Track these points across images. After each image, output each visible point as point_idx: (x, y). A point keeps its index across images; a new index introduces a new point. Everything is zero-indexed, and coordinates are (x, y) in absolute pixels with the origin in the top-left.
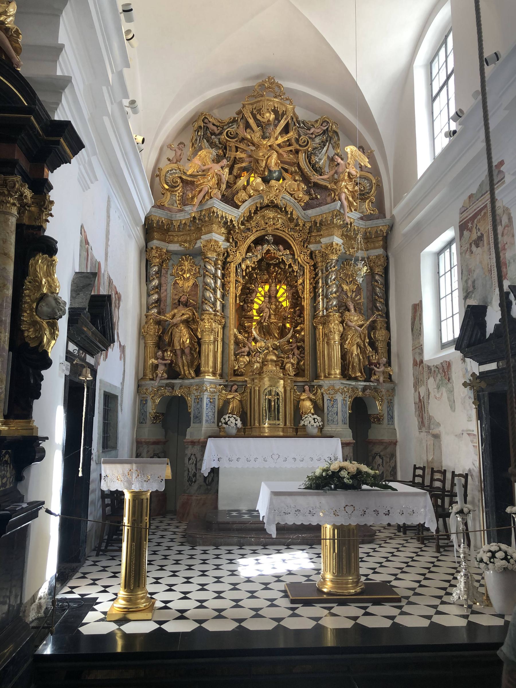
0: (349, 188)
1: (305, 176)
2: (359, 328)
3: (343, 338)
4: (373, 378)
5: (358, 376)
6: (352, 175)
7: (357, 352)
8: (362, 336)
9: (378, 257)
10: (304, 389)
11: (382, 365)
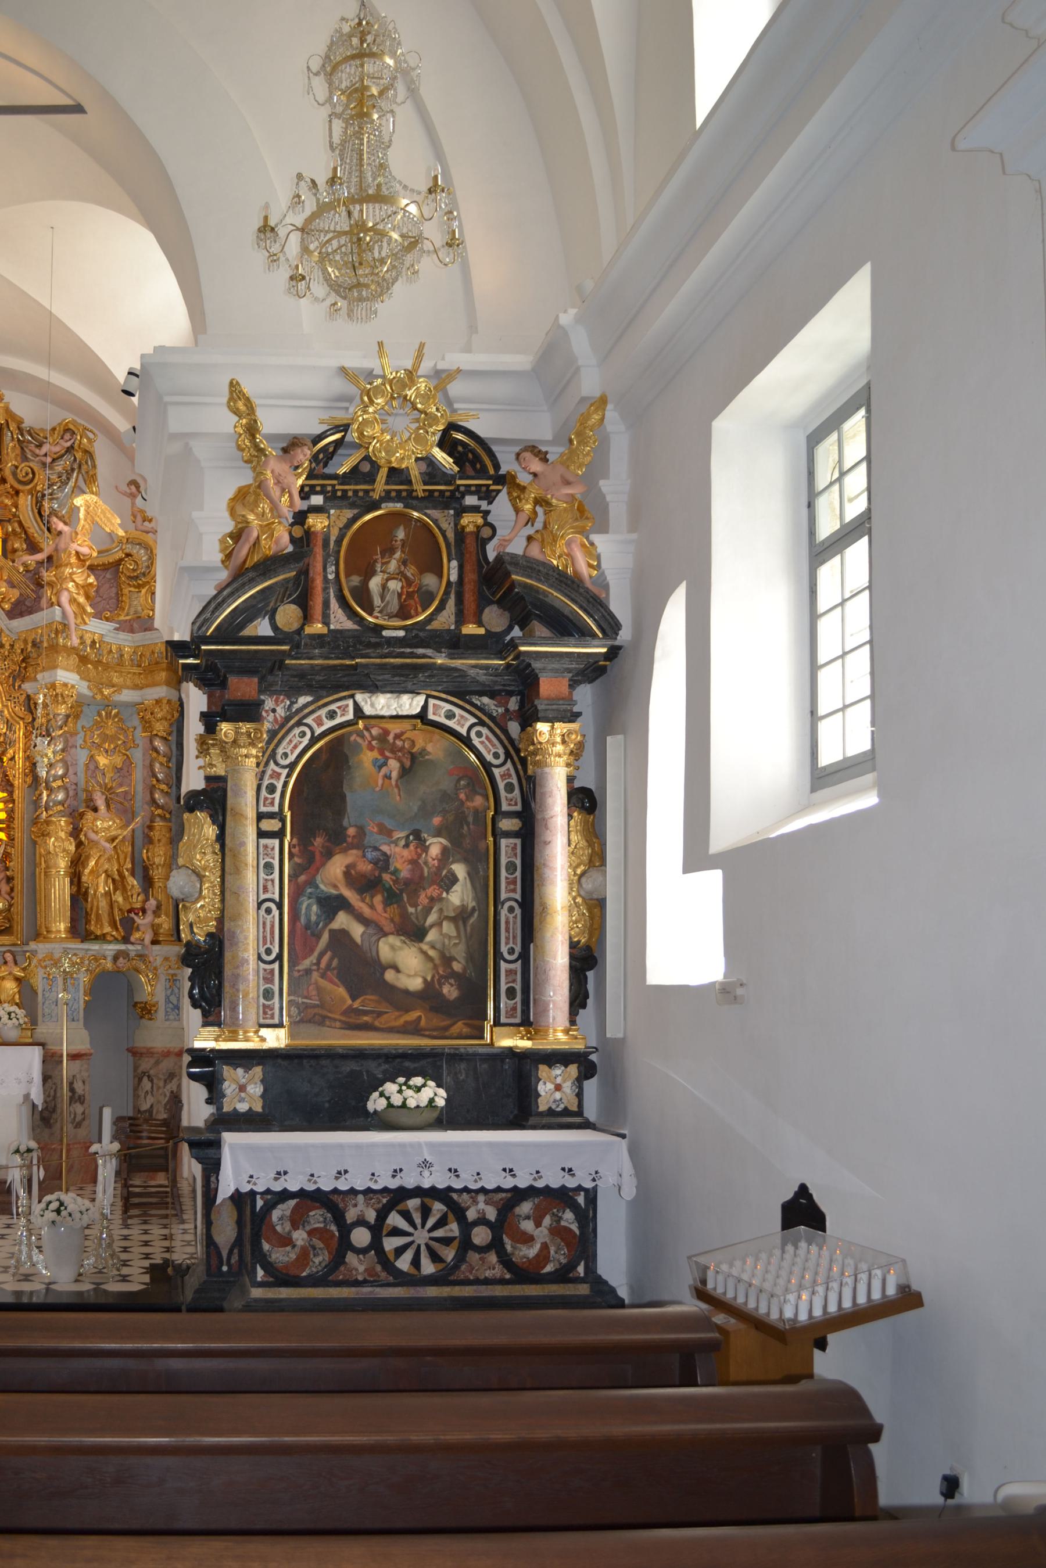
0: (77, 580)
1: (31, 541)
2: (107, 845)
3: (77, 863)
4: (136, 935)
5: (107, 933)
6: (84, 555)
7: (104, 889)
8: (122, 857)
9: (158, 702)
10: (4, 958)
11: (149, 913)
